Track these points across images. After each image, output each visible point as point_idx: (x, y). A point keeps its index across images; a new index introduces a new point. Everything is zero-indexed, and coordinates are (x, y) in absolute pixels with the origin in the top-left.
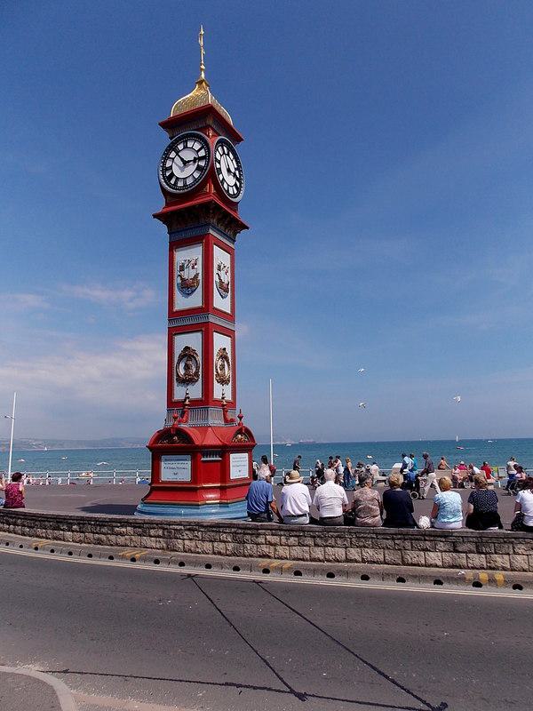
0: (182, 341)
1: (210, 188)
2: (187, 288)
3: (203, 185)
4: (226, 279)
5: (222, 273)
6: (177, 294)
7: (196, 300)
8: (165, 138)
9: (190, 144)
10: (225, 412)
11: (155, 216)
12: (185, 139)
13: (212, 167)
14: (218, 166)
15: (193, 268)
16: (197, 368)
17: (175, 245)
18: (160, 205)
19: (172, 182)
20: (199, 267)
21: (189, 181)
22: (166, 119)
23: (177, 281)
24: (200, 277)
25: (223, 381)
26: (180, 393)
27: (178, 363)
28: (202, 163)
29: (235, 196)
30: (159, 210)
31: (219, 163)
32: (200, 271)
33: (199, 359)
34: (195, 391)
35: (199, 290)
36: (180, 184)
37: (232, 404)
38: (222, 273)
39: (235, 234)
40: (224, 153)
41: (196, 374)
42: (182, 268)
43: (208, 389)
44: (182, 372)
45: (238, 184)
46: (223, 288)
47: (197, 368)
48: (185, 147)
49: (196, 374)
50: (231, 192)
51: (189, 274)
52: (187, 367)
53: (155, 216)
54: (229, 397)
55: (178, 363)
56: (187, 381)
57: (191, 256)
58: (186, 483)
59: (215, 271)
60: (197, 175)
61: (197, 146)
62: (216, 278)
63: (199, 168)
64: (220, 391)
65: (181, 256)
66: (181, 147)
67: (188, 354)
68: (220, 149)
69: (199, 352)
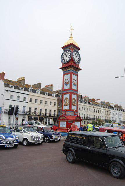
2: (67, 84)
3: (69, 61)
4: (75, 82)
5: (74, 81)
6: (65, 85)
7: (68, 87)
8: (62, 51)
10: (74, 113)
11: (60, 68)
13: (72, 57)
14: (73, 56)
17: (64, 75)
18: (61, 65)
20: (69, 80)
21: (67, 60)
22: (63, 47)
23: (65, 83)
24: (69, 82)
25: (74, 105)
26: (65, 108)
27: (65, 100)
28: (70, 56)
29: (78, 63)
30: (61, 67)
31: (74, 56)
32: (69, 81)
34: (68, 108)
35: (69, 85)
36: (65, 61)
37: (77, 111)
38: (74, 81)
39: (78, 71)
41: (68, 104)
42: (65, 80)
43: (70, 107)
44: (65, 103)
45: (79, 59)
46: (75, 85)
49: (68, 104)
50: (77, 62)
51: (67, 81)
52: (66, 102)
54: (76, 109)
55: (64, 101)
56: (66, 105)
57: (68, 77)
58: (64, 128)
59: (73, 80)
62: (73, 82)
63: (69, 57)
64: (73, 108)
65: (66, 77)
66: (65, 53)
68: (74, 53)
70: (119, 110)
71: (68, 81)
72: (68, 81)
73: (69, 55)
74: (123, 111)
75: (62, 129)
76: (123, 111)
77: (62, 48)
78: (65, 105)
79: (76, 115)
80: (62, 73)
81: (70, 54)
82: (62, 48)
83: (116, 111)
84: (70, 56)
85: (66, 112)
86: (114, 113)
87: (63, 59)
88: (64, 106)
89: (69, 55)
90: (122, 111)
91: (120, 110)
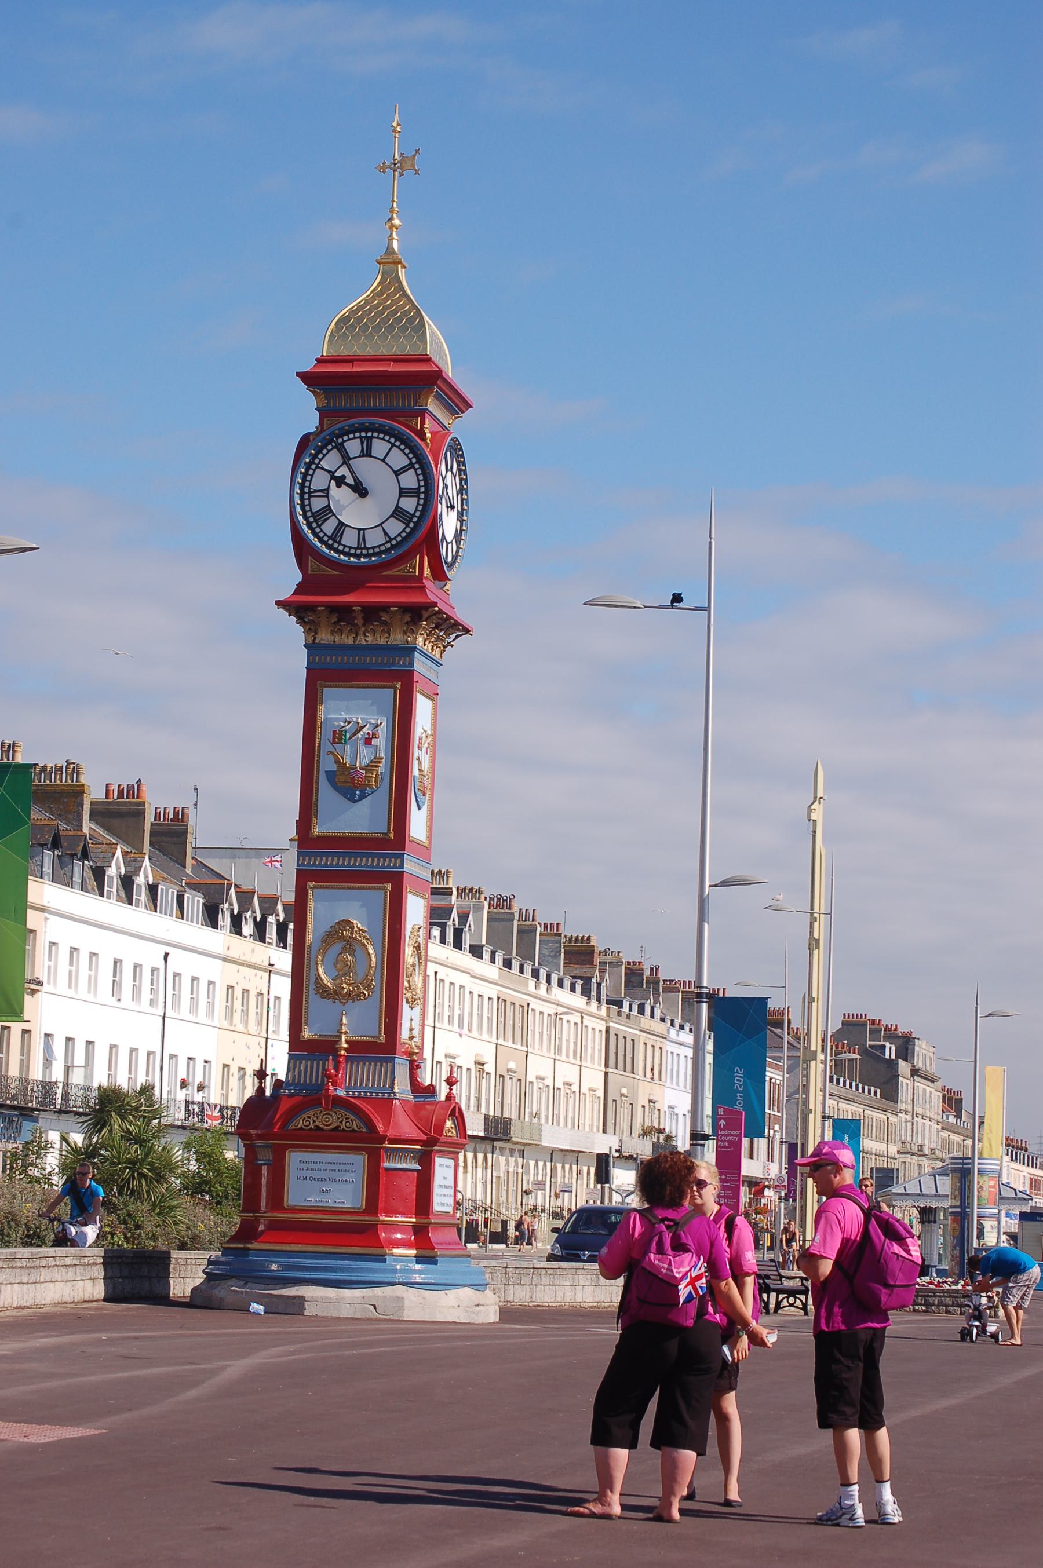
6: (325, 793)
8: (305, 413)
9: (379, 447)
11: (280, 604)
12: (367, 433)
15: (368, 741)
19: (329, 527)
21: (375, 539)
23: (327, 764)
30: (287, 592)
36: (349, 539)
40: (447, 470)
48: (367, 453)
53: (280, 604)
60: (395, 528)
61: (399, 459)
63: (398, 513)
70: (168, 892)
71: (376, 761)
72: (376, 761)
73: (403, 492)
79: (431, 1090)
80: (299, 660)
81: (409, 480)
83: (137, 917)
84: (409, 504)
86: (110, 947)
87: (317, 504)
90: (211, 917)
91: (195, 902)
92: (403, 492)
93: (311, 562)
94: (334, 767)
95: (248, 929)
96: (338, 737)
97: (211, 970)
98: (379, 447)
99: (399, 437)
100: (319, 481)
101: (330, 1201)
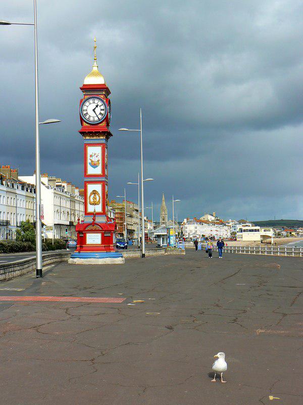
0: (91, 188)
1: (104, 124)
2: (94, 166)
8: (81, 95)
16: (100, 199)
19: (87, 117)
20: (100, 157)
22: (81, 86)
23: (89, 161)
24: (100, 162)
26: (91, 209)
28: (103, 112)
33: (101, 195)
34: (99, 208)
44: (92, 200)
47: (100, 199)
51: (95, 159)
52: (94, 198)
56: (95, 204)
65: (91, 150)
67: (94, 192)
69: (100, 192)
72: (98, 161)
74: (27, 191)
75: (94, 248)
76: (27, 191)
77: (81, 89)
78: (91, 204)
82: (81, 89)
84: (103, 112)
85: (94, 217)
87: (85, 112)
88: (89, 205)
89: (101, 110)
91: (20, 187)
92: (101, 110)
93: (85, 124)
94: (90, 162)
95: (29, 191)
96: (91, 156)
97: (23, 198)
98: (96, 101)
99: (99, 99)
100: (85, 108)
101: (95, 243)
